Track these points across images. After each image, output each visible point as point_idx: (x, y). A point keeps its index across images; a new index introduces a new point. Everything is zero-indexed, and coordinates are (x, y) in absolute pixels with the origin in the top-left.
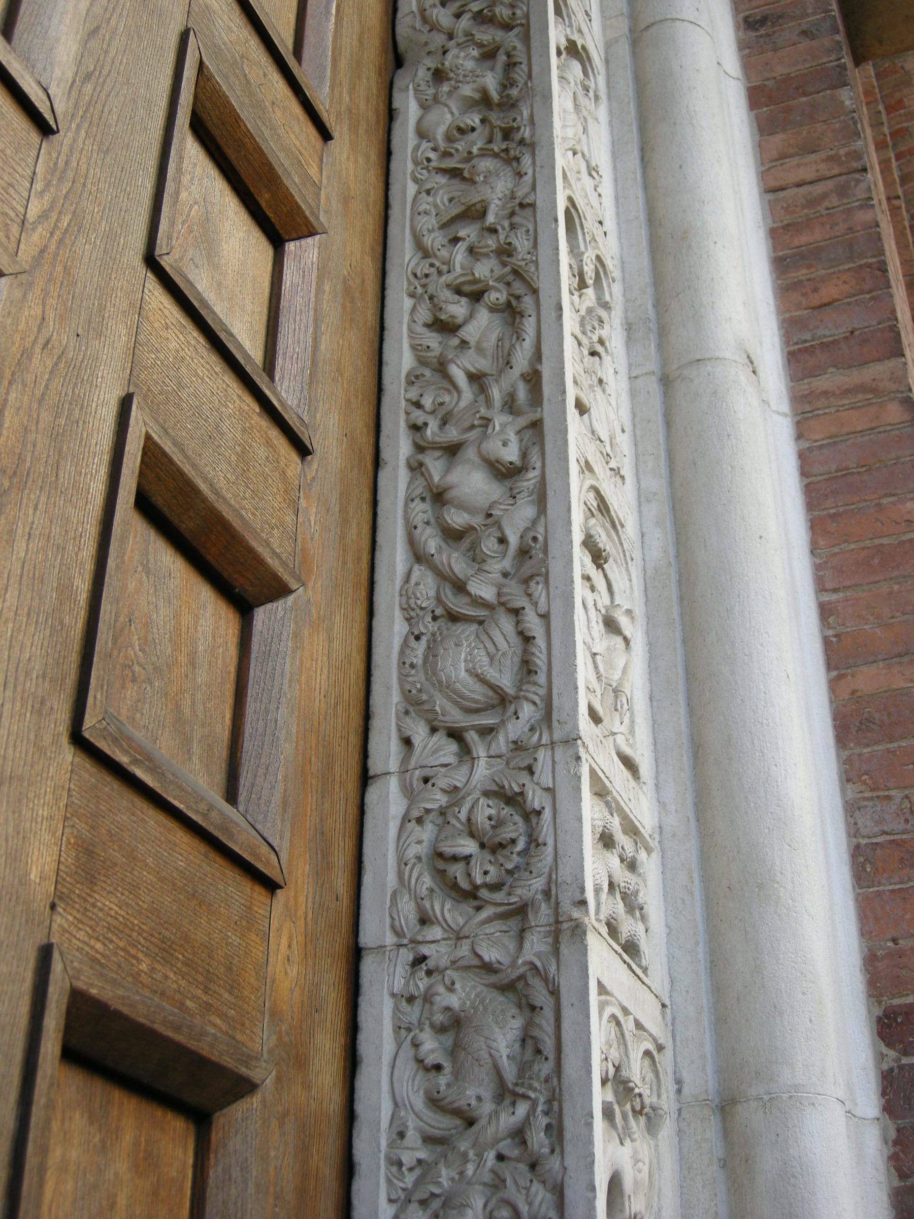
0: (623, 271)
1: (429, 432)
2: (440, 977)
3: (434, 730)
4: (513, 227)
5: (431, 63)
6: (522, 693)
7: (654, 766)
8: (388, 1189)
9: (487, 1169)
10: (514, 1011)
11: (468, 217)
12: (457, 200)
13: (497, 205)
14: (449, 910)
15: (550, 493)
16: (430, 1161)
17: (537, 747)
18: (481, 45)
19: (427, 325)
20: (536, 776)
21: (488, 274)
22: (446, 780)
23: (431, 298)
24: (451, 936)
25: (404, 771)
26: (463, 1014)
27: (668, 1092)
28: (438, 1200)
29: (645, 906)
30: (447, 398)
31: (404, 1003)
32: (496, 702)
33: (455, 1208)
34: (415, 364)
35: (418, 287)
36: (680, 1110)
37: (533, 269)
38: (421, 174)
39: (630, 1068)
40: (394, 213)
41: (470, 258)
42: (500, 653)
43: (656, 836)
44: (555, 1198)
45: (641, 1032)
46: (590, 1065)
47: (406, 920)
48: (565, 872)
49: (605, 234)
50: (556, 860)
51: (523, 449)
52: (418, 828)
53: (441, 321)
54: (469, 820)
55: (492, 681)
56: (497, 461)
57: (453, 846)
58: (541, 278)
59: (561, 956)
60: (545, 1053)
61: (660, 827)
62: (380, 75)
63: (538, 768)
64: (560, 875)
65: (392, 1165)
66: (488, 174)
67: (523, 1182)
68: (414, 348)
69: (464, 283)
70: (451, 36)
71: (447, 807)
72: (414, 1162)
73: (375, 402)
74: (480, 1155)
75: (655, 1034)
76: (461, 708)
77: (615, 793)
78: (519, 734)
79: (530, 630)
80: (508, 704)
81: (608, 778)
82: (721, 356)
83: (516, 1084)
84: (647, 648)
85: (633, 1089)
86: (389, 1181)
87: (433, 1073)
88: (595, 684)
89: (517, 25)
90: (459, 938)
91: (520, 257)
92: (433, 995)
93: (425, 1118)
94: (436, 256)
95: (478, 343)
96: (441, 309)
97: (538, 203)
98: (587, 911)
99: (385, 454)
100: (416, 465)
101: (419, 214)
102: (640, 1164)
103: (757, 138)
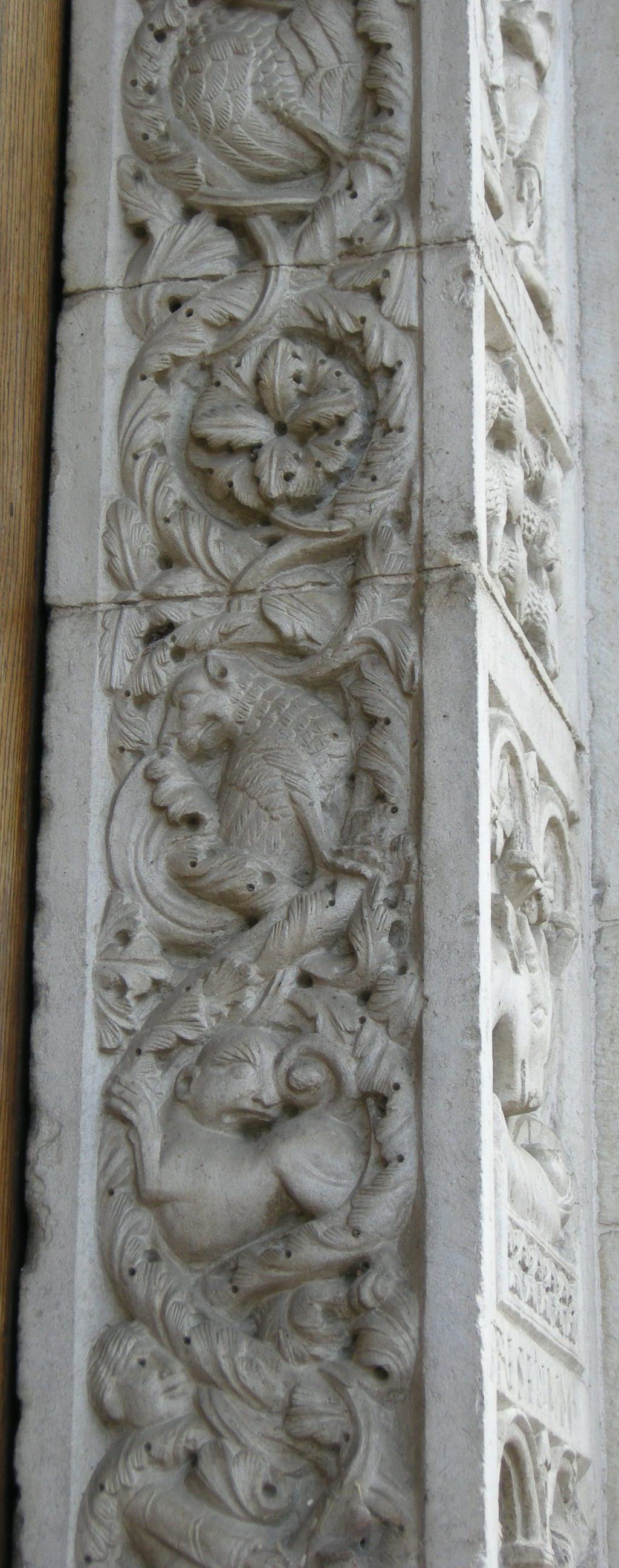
2: (198, 662)
3: (190, 212)
6: (363, 150)
7: (577, 314)
8: (99, 1031)
9: (281, 1001)
10: (337, 725)
14: (218, 542)
16: (175, 983)
17: (390, 251)
20: (387, 304)
22: (216, 305)
24: (220, 588)
25: (132, 285)
26: (240, 728)
27: (580, 898)
28: (190, 1050)
29: (557, 565)
31: (130, 705)
32: (310, 163)
33: (220, 1065)
36: (599, 933)
39: (529, 842)
42: (321, 72)
43: (576, 439)
44: (405, 1049)
45: (545, 786)
46: (477, 823)
47: (137, 556)
48: (437, 481)
50: (421, 459)
52: (159, 392)
54: (257, 380)
55: (307, 124)
57: (227, 427)
59: (427, 630)
60: (392, 800)
61: (583, 427)
63: (390, 291)
64: (428, 485)
65: (107, 989)
67: (349, 1023)
71: (215, 355)
72: (146, 986)
74: (270, 976)
75: (565, 792)
76: (244, 173)
77: (520, 351)
78: (355, 225)
79: (380, 30)
80: (334, 171)
81: (510, 320)
83: (338, 853)
84: (572, 91)
85: (532, 880)
86: (101, 1016)
87: (183, 832)
88: (493, 145)
90: (234, 593)
92: (185, 693)
93: (167, 908)
98: (476, 553)
102: (540, 1012)
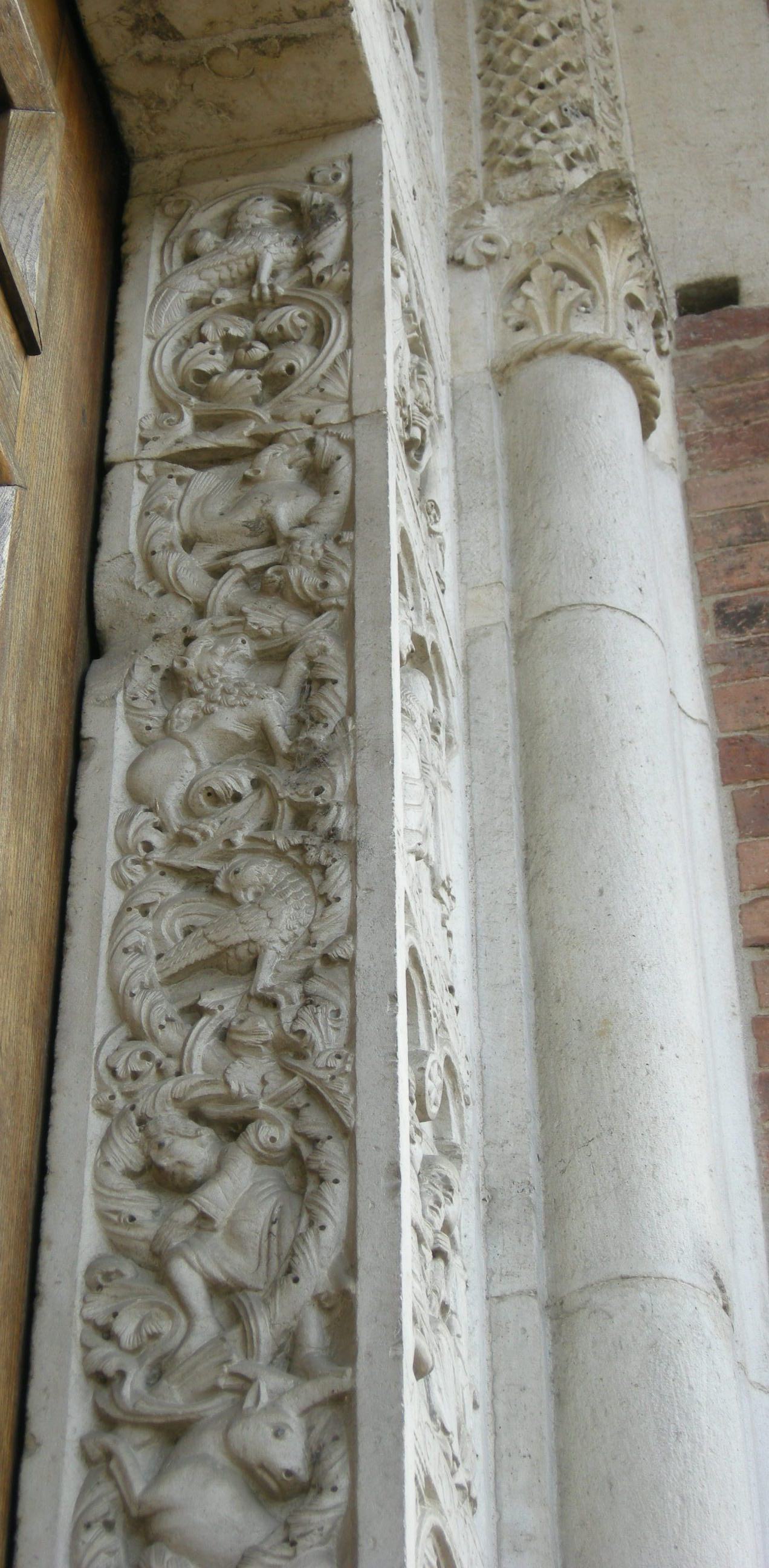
0: (482, 1083)
1: (127, 1391)
4: (308, 1000)
5: (160, 656)
11: (219, 967)
12: (200, 932)
13: (279, 953)
15: (365, 1545)
18: (260, 637)
19: (130, 1174)
21: (256, 1088)
23: (142, 1121)
30: (165, 1326)
34: (105, 1249)
35: (118, 1096)
37: (345, 1089)
38: (131, 873)
40: (78, 940)
41: (222, 1052)
49: (457, 1009)
51: (315, 1448)
53: (160, 1169)
56: (262, 1466)
58: (359, 1109)
62: (65, 671)
66: (264, 893)
68: (103, 1216)
69: (207, 1099)
70: (200, 611)
73: (22, 1317)
82: (667, 1273)
89: (330, 607)
91: (321, 1062)
94: (154, 1039)
95: (232, 1223)
96: (161, 1145)
97: (361, 961)
99: (37, 1425)
100: (97, 1453)
101: (126, 951)
103: (734, 839)
